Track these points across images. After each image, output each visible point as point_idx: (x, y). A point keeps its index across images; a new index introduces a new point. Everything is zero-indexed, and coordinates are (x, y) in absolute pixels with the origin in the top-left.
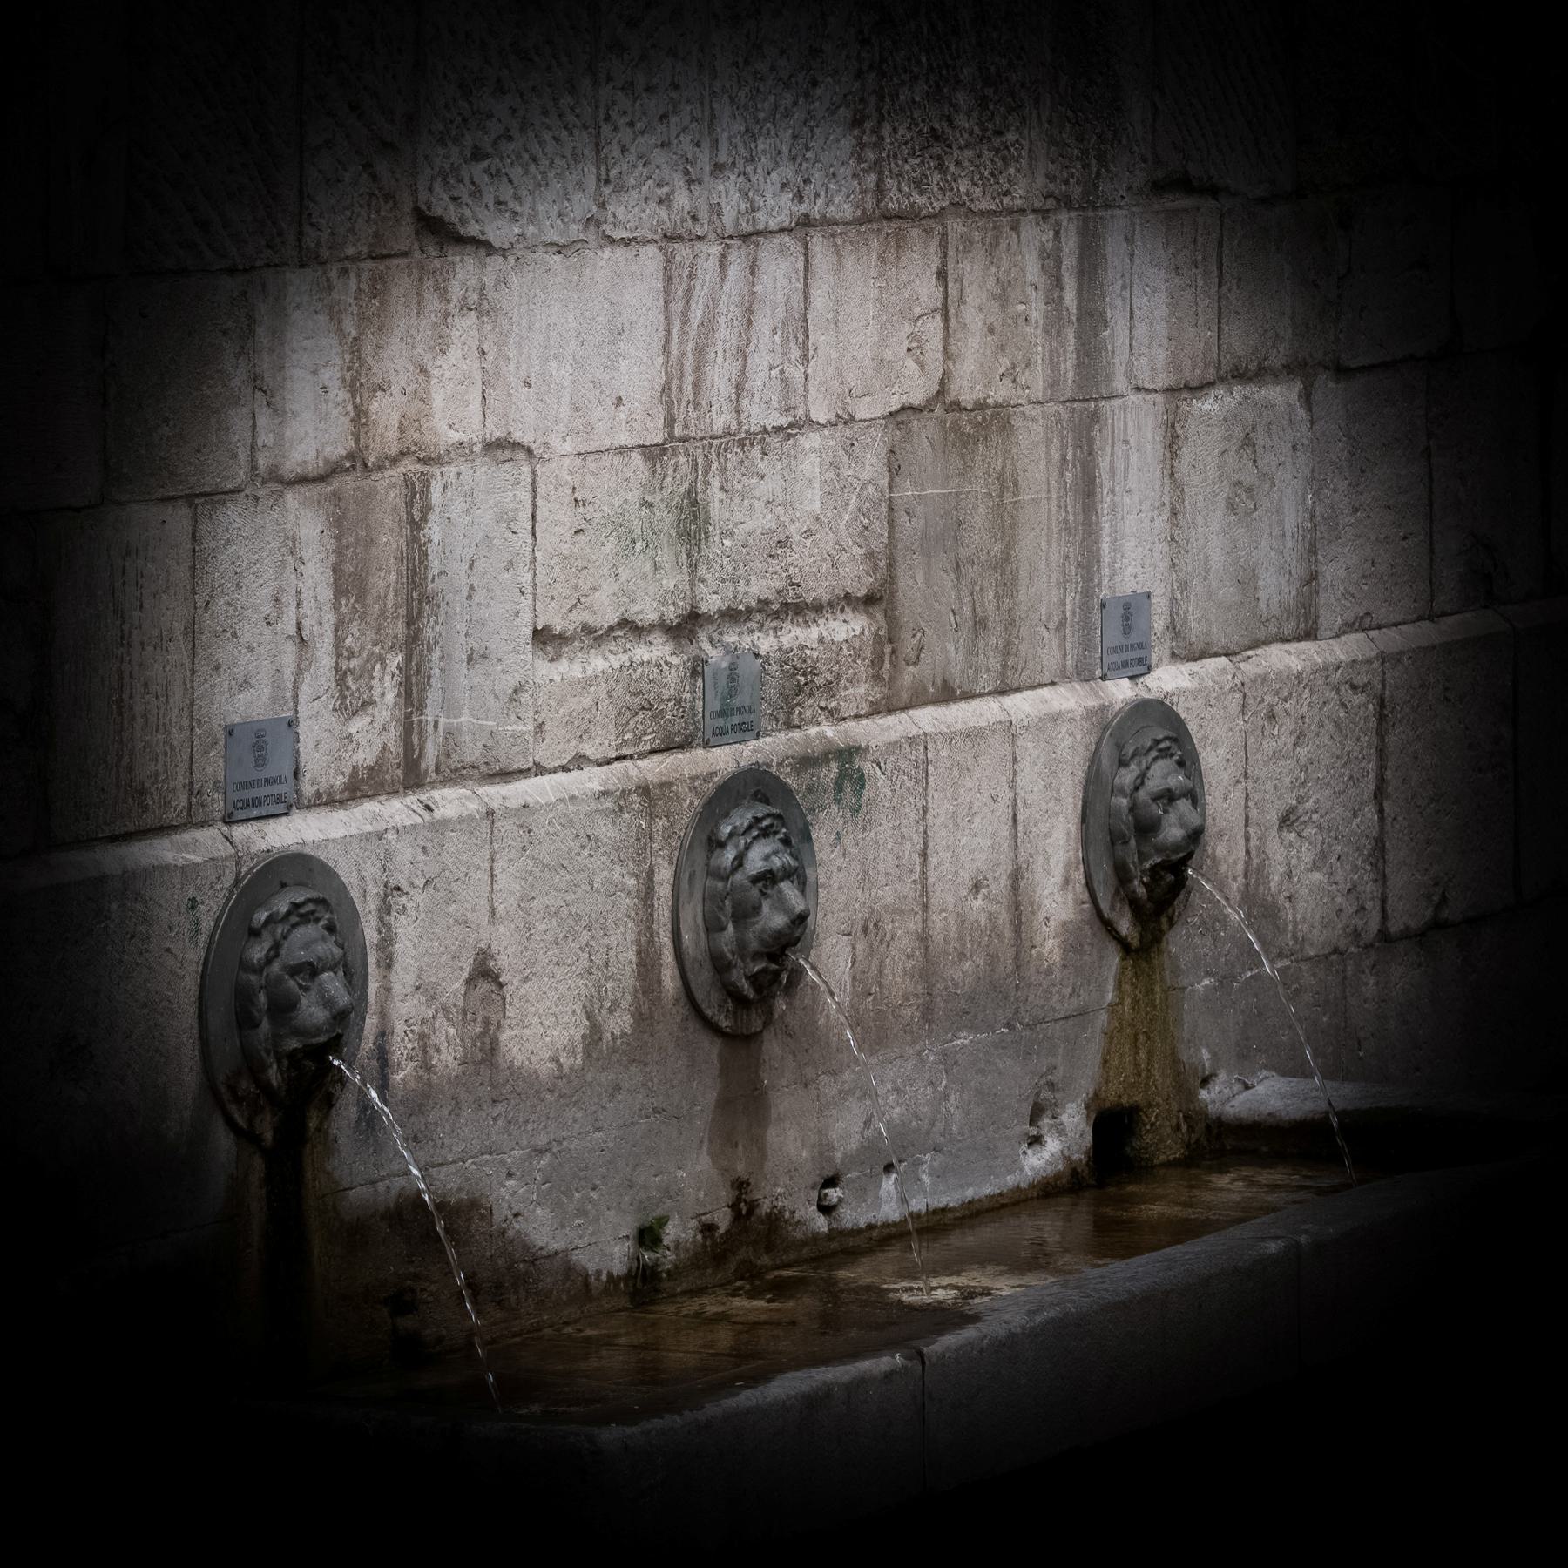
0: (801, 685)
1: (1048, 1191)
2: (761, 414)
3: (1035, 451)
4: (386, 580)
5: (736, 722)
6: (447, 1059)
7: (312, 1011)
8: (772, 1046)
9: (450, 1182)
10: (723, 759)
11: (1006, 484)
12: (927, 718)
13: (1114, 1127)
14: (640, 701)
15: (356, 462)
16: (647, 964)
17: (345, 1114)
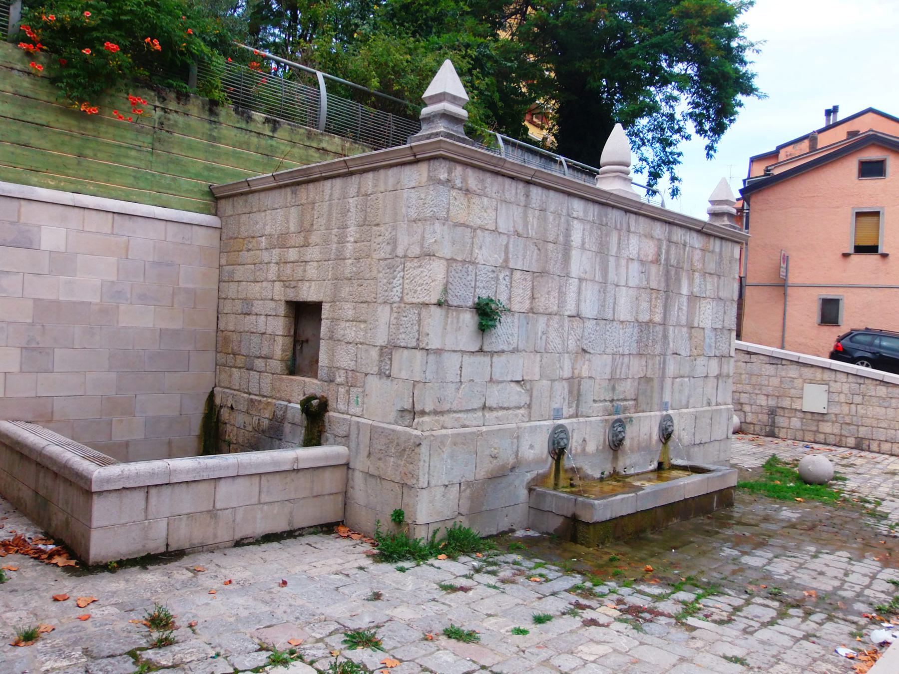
0: (626, 409)
1: (652, 471)
2: (623, 377)
3: (656, 384)
4: (575, 392)
5: (617, 413)
6: (579, 450)
7: (562, 444)
8: (619, 452)
9: (578, 466)
10: (616, 417)
11: (652, 387)
12: (641, 414)
13: (660, 465)
14: (606, 409)
15: (572, 378)
16: (605, 441)
17: (565, 456)
